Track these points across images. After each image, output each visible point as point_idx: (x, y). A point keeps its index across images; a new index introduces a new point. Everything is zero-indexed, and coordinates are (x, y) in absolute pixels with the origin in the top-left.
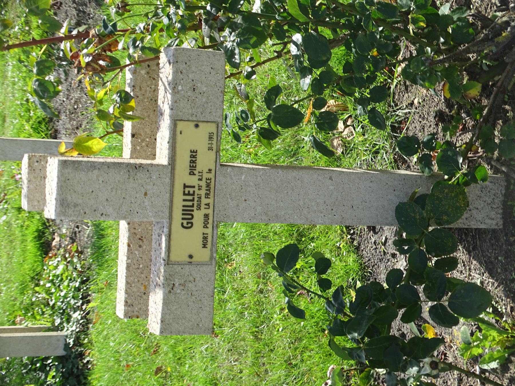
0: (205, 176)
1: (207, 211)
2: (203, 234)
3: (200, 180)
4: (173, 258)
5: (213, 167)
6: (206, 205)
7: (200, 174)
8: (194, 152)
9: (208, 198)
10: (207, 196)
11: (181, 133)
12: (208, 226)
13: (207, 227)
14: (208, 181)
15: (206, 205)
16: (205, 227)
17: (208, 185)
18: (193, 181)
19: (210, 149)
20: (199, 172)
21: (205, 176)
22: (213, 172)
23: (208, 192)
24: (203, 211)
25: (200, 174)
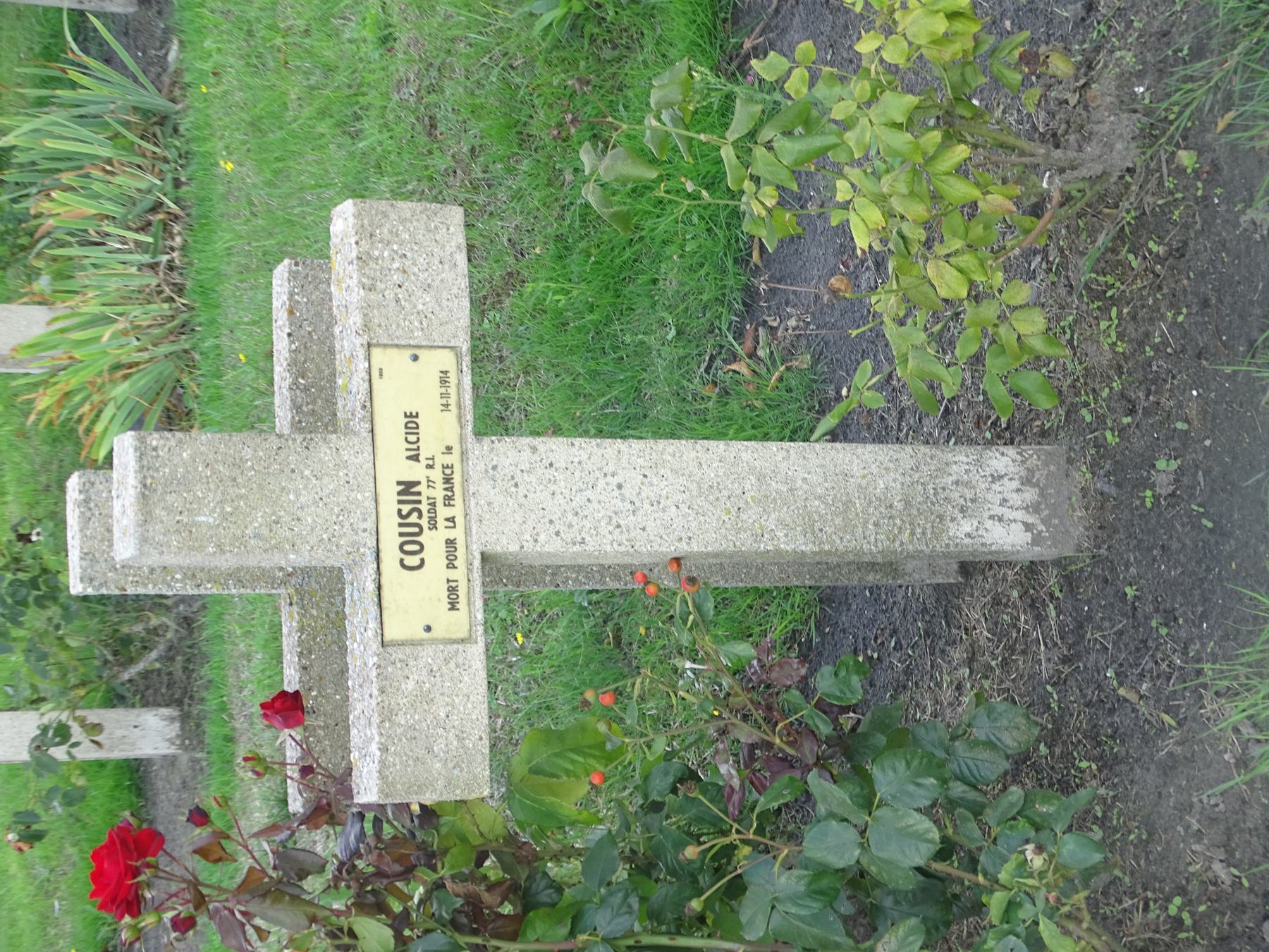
1: (451, 534)
2: (448, 581)
4: (389, 636)
6: (447, 520)
8: (411, 416)
9: (449, 505)
10: (448, 501)
11: (381, 375)
12: (456, 563)
13: (455, 567)
14: (448, 471)
15: (447, 520)
16: (451, 566)
17: (448, 480)
18: (416, 472)
21: (441, 460)
23: (450, 494)
24: (443, 533)
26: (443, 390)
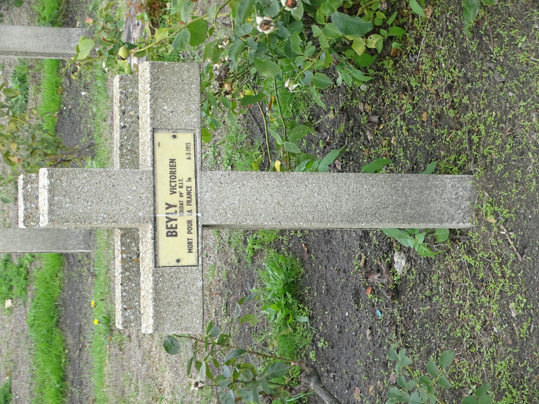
0: (186, 184)
2: (188, 239)
3: (181, 187)
5: (192, 176)
6: (188, 211)
7: (181, 182)
9: (189, 205)
10: (189, 203)
11: (159, 145)
14: (189, 189)
15: (188, 211)
16: (189, 232)
17: (189, 193)
19: (189, 158)
20: (179, 180)
22: (193, 180)
23: (190, 200)
25: (181, 182)
26: (188, 152)
